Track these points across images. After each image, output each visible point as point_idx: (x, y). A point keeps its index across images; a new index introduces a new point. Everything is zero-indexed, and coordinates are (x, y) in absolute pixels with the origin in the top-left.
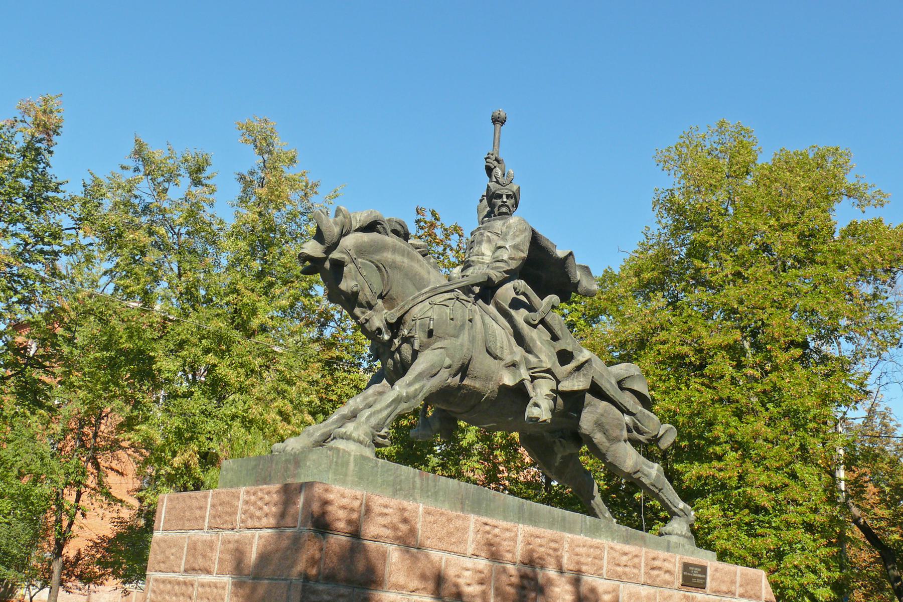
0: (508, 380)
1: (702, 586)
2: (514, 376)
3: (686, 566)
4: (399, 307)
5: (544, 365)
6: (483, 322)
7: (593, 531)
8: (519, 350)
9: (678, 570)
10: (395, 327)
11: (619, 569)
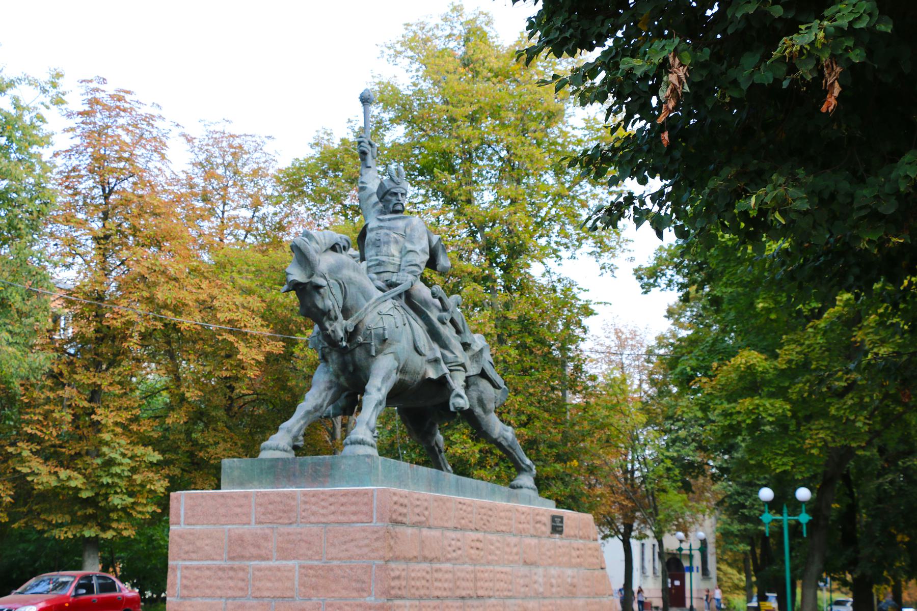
0: (432, 374)
1: (561, 532)
2: (437, 370)
3: (554, 518)
4: (355, 317)
5: (459, 360)
6: (410, 324)
7: (436, 486)
8: (436, 346)
9: (547, 520)
10: (351, 336)
11: (520, 526)
